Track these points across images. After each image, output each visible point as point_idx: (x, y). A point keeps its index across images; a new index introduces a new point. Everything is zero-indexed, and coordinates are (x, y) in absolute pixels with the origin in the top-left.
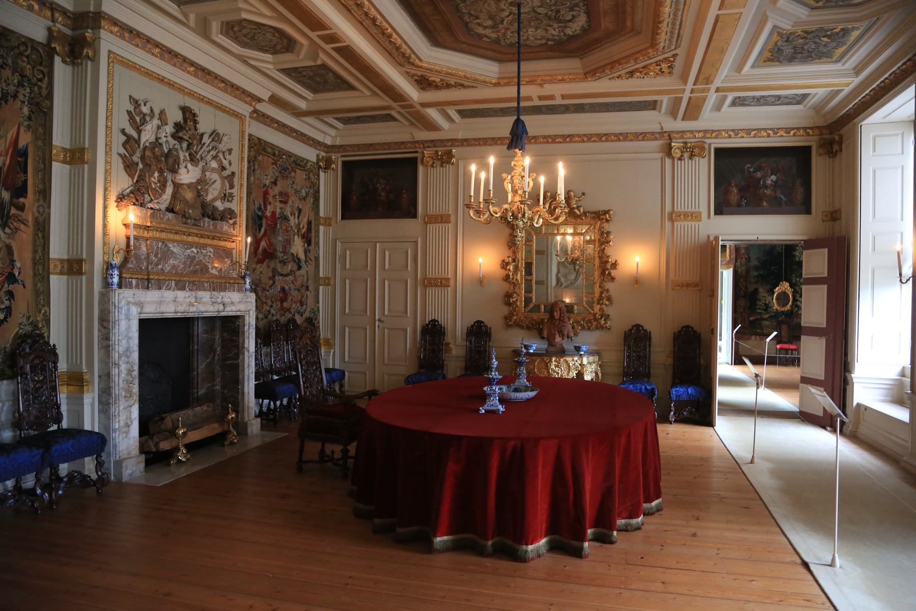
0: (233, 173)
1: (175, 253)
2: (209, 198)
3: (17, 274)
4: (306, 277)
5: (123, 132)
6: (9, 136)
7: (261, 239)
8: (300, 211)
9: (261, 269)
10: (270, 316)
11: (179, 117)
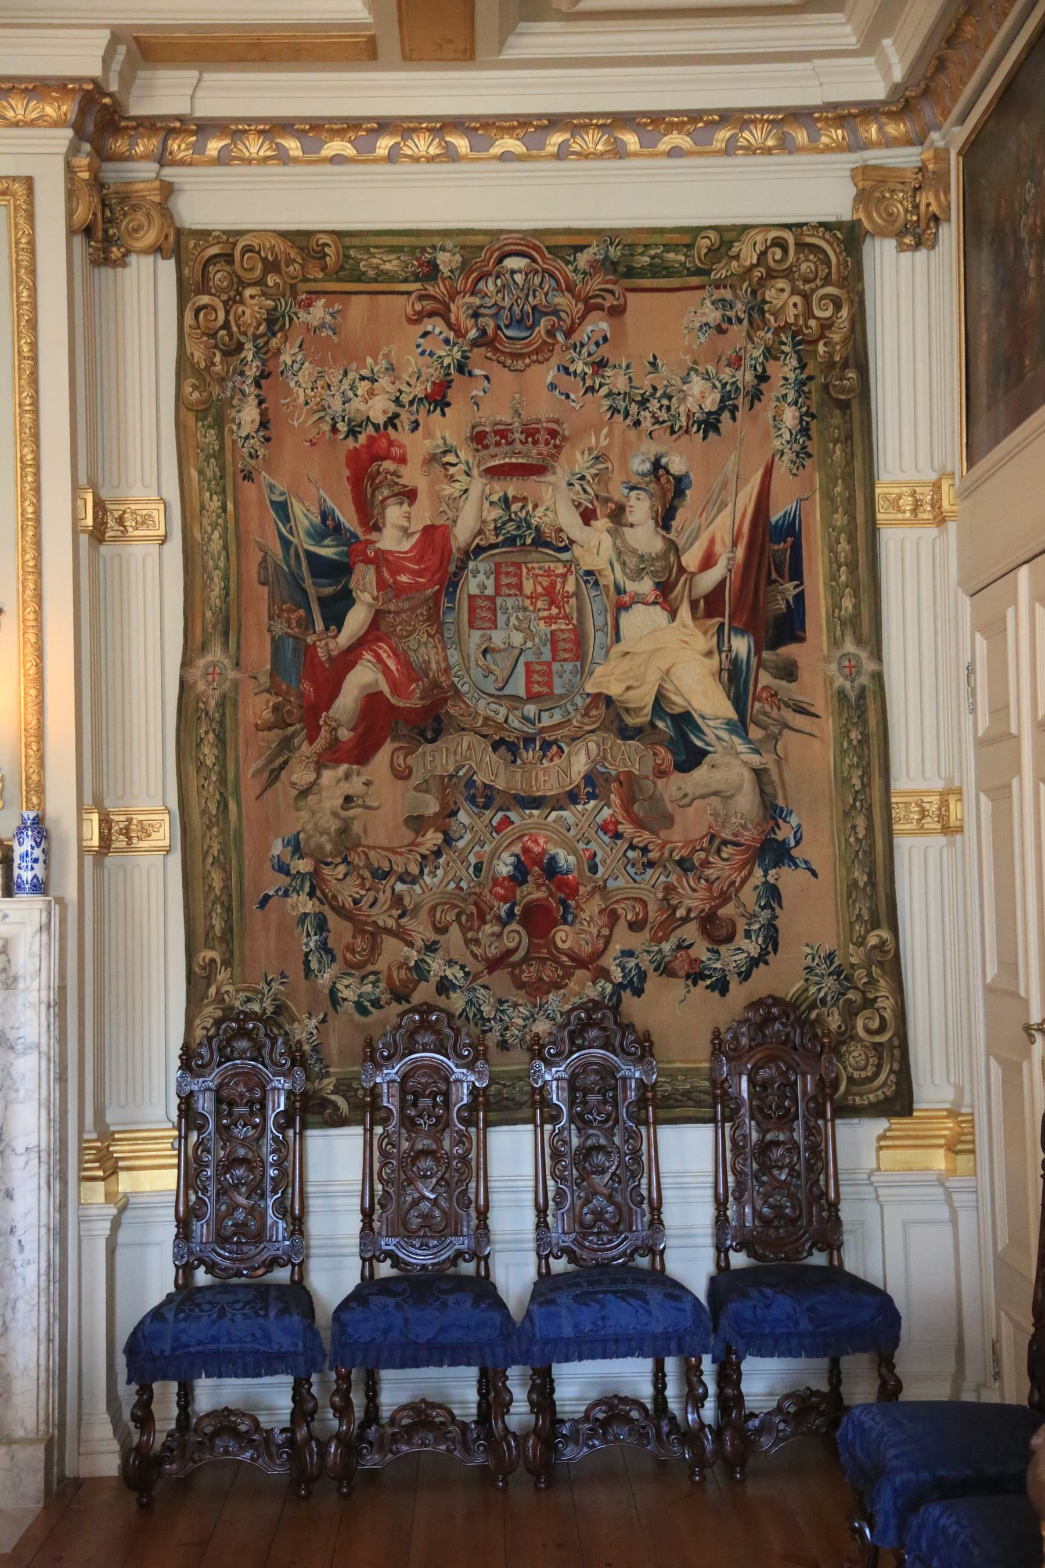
4: (746, 802)
7: (348, 659)
9: (355, 786)
10: (424, 993)
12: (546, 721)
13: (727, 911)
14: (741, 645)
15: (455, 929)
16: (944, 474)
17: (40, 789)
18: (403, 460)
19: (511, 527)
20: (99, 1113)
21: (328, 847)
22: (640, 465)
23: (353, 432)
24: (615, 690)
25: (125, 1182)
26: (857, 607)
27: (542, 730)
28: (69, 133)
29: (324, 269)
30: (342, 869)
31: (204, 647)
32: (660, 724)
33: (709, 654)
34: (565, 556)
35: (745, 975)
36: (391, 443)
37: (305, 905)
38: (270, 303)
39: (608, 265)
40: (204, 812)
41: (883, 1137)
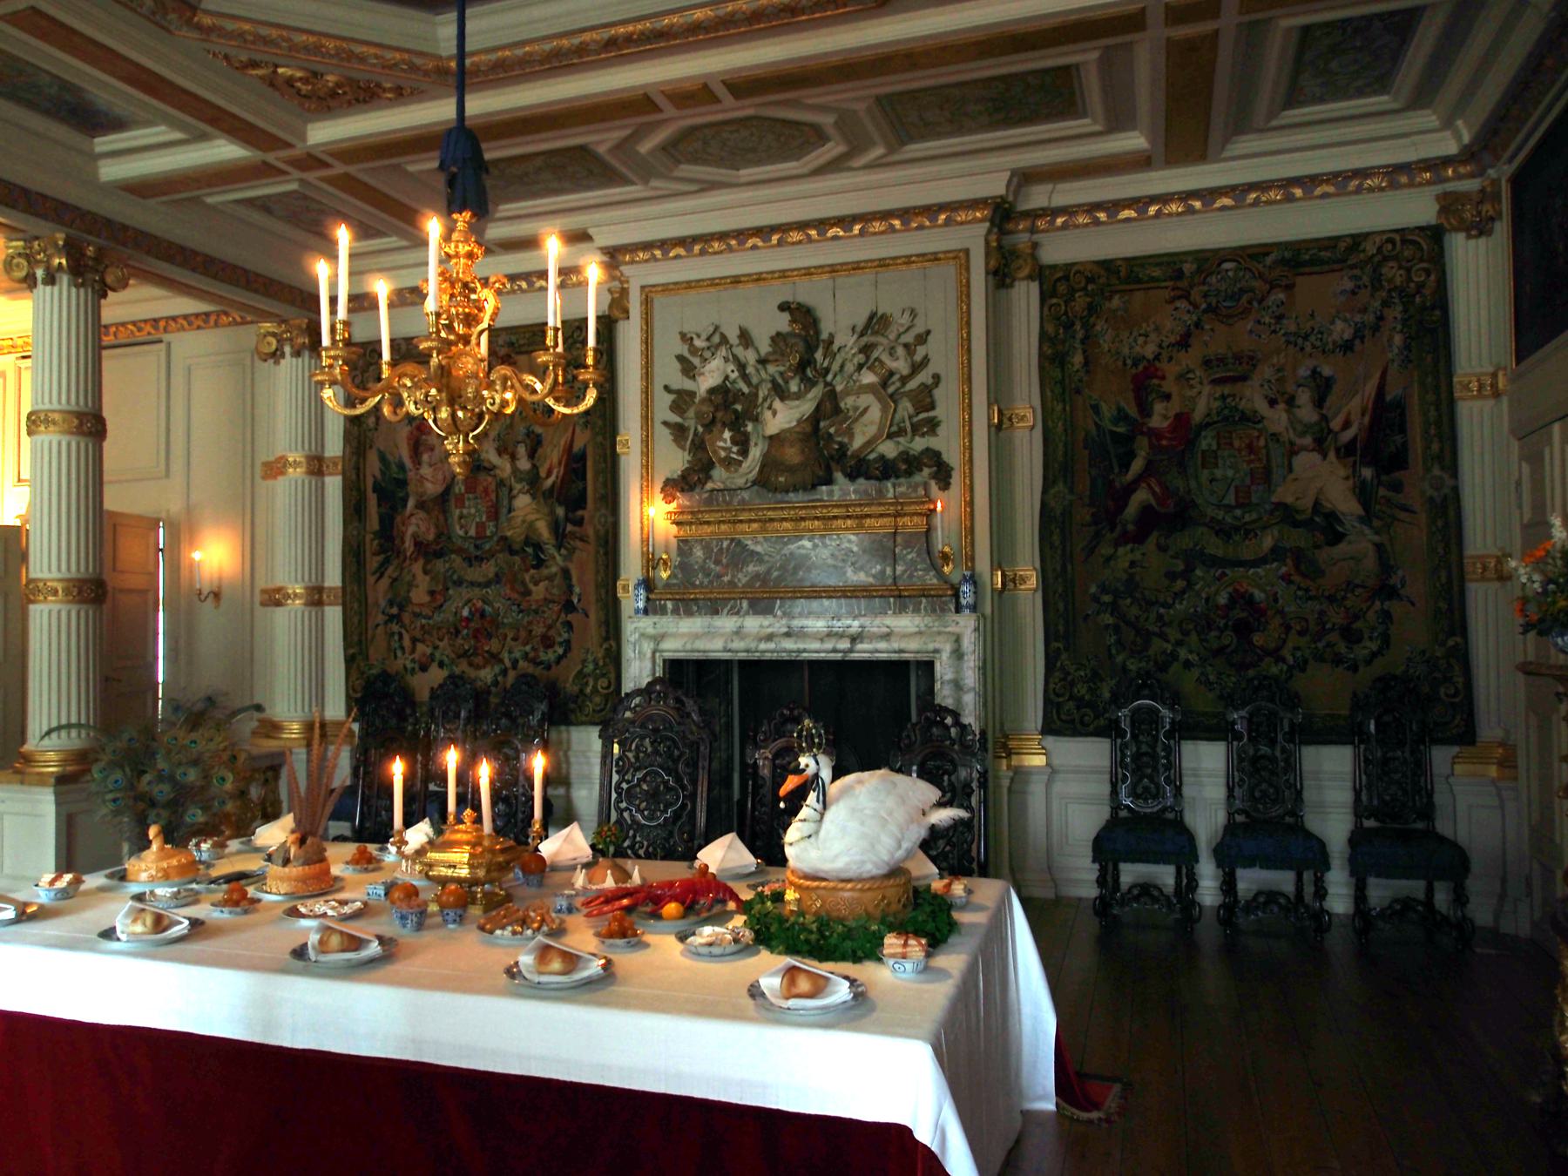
0: (937, 378)
1: (758, 553)
2: (858, 443)
3: (575, 601)
4: (1370, 563)
5: (666, 388)
6: (562, 443)
8: (1322, 388)
9: (1137, 556)
11: (783, 323)
12: (1247, 518)
13: (1358, 625)
14: (1367, 473)
15: (1194, 633)
16: (1498, 368)
17: (973, 559)
18: (1163, 378)
19: (1226, 412)
20: (1002, 725)
21: (1122, 589)
22: (1303, 372)
23: (1135, 364)
24: (1289, 500)
25: (1015, 761)
26: (1442, 450)
27: (1246, 523)
28: (987, 224)
29: (1119, 278)
30: (1129, 601)
31: (1054, 482)
32: (1317, 519)
33: (1347, 478)
34: (1260, 426)
35: (1369, 662)
36: (1157, 370)
37: (1108, 619)
38: (1088, 299)
39: (1283, 262)
40: (1054, 570)
41: (1457, 757)
